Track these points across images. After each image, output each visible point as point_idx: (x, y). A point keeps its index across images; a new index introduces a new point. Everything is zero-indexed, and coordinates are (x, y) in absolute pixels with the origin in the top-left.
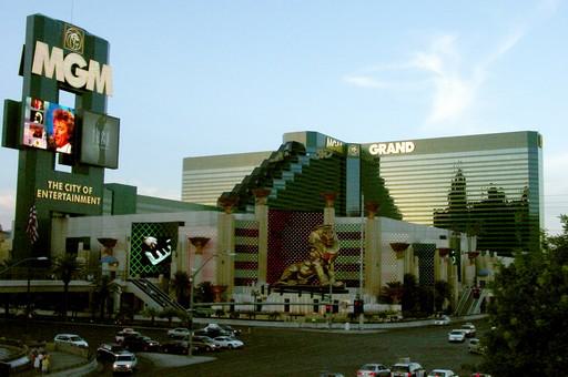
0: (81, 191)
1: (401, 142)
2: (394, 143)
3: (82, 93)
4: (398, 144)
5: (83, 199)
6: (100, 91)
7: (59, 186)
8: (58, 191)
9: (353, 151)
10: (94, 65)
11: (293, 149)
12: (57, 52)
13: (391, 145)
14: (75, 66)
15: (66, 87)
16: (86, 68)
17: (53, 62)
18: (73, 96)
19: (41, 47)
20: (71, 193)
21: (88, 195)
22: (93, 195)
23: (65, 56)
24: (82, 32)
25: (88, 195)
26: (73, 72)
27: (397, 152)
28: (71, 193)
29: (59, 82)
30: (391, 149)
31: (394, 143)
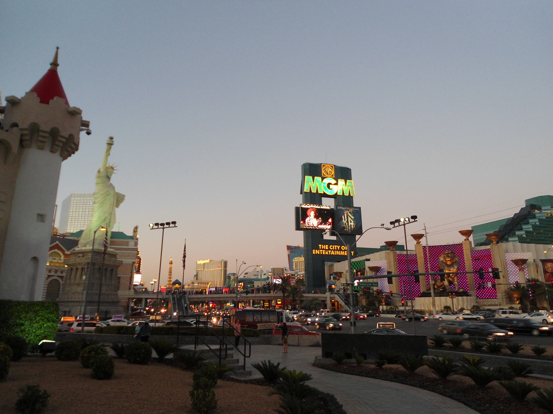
0: (340, 248)
3: (335, 196)
5: (342, 253)
6: (347, 194)
7: (326, 247)
10: (341, 182)
14: (329, 184)
15: (325, 195)
16: (336, 184)
17: (317, 184)
19: (308, 178)
20: (334, 250)
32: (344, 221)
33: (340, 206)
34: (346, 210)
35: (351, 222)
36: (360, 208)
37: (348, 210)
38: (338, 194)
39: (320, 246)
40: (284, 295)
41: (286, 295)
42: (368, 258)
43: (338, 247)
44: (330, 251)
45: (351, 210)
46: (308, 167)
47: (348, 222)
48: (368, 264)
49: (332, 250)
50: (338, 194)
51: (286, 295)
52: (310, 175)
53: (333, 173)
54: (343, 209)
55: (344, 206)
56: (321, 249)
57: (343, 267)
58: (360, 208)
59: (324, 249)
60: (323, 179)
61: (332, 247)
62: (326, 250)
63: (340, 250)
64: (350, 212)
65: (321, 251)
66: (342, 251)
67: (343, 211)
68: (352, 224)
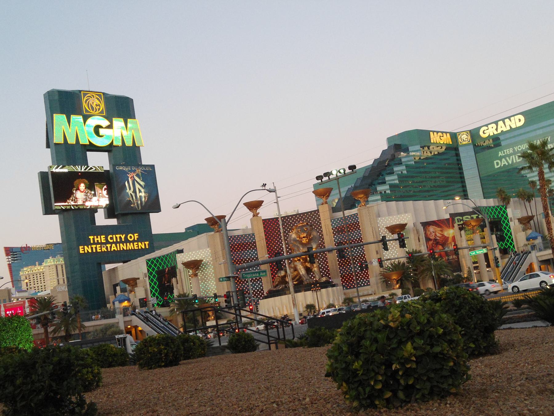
0: (126, 238)
1: (509, 118)
2: (503, 120)
3: (109, 149)
4: (507, 121)
5: (130, 246)
6: (129, 143)
8: (103, 243)
9: (464, 138)
10: (118, 123)
11: (397, 146)
12: (77, 119)
13: (501, 123)
14: (97, 129)
16: (110, 127)
17: (75, 129)
18: (105, 156)
19: (59, 119)
20: (116, 243)
21: (134, 241)
22: (140, 240)
23: (85, 123)
24: (99, 94)
25: (134, 241)
26: (97, 132)
27: (508, 128)
28: (116, 243)
29: (85, 146)
30: (502, 128)
31: (503, 120)
32: (130, 192)
33: (120, 165)
34: (131, 171)
35: (140, 191)
36: (153, 167)
37: (134, 171)
38: (115, 144)
39: (91, 237)
40: (46, 331)
41: (50, 329)
42: (180, 248)
43: (123, 237)
44: (109, 246)
45: (139, 171)
46: (57, 97)
47: (135, 191)
48: (181, 259)
49: (111, 243)
50: (115, 144)
51: (50, 329)
52: (62, 112)
53: (102, 106)
54: (125, 169)
55: (126, 165)
56: (94, 243)
57: (138, 268)
58: (153, 167)
59: (98, 243)
60: (85, 118)
61: (112, 238)
62: (101, 243)
63: (127, 241)
64: (138, 175)
65: (94, 246)
66: (130, 242)
67: (126, 173)
68: (143, 194)
